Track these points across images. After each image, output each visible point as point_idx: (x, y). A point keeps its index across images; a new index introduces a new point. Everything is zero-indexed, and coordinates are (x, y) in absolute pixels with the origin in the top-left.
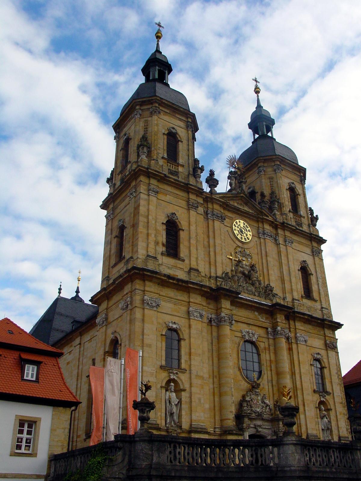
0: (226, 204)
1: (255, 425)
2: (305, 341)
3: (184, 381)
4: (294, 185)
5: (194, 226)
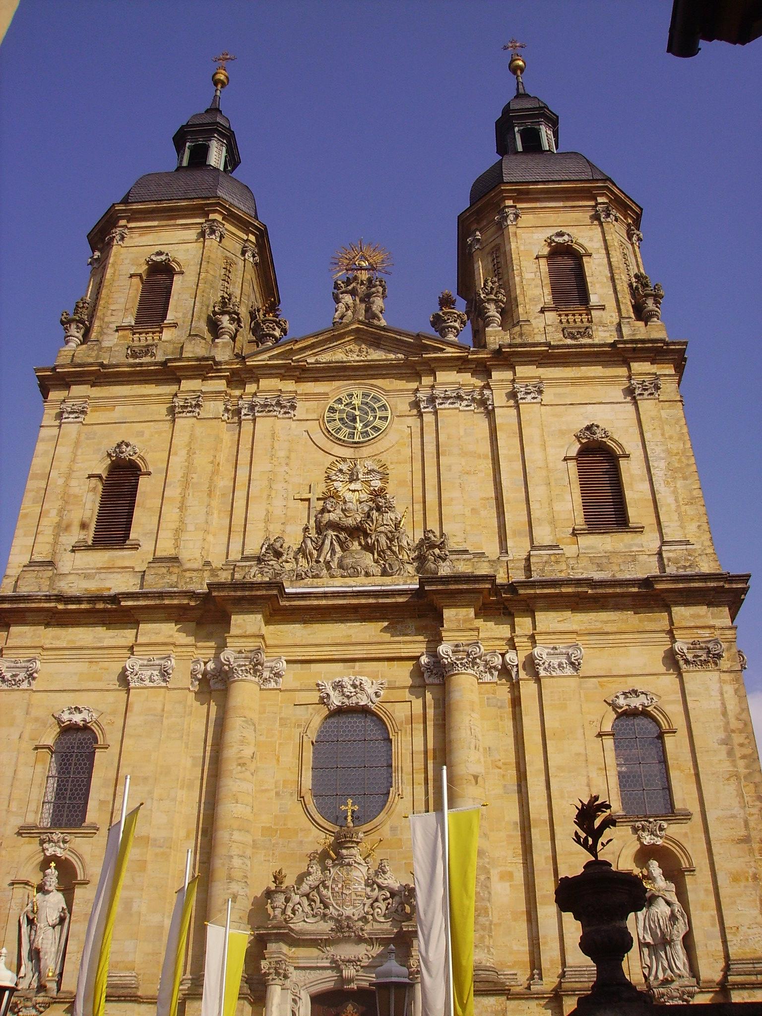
1: (334, 961)
2: (572, 664)
3: (87, 858)
4: (566, 238)
5: (183, 453)
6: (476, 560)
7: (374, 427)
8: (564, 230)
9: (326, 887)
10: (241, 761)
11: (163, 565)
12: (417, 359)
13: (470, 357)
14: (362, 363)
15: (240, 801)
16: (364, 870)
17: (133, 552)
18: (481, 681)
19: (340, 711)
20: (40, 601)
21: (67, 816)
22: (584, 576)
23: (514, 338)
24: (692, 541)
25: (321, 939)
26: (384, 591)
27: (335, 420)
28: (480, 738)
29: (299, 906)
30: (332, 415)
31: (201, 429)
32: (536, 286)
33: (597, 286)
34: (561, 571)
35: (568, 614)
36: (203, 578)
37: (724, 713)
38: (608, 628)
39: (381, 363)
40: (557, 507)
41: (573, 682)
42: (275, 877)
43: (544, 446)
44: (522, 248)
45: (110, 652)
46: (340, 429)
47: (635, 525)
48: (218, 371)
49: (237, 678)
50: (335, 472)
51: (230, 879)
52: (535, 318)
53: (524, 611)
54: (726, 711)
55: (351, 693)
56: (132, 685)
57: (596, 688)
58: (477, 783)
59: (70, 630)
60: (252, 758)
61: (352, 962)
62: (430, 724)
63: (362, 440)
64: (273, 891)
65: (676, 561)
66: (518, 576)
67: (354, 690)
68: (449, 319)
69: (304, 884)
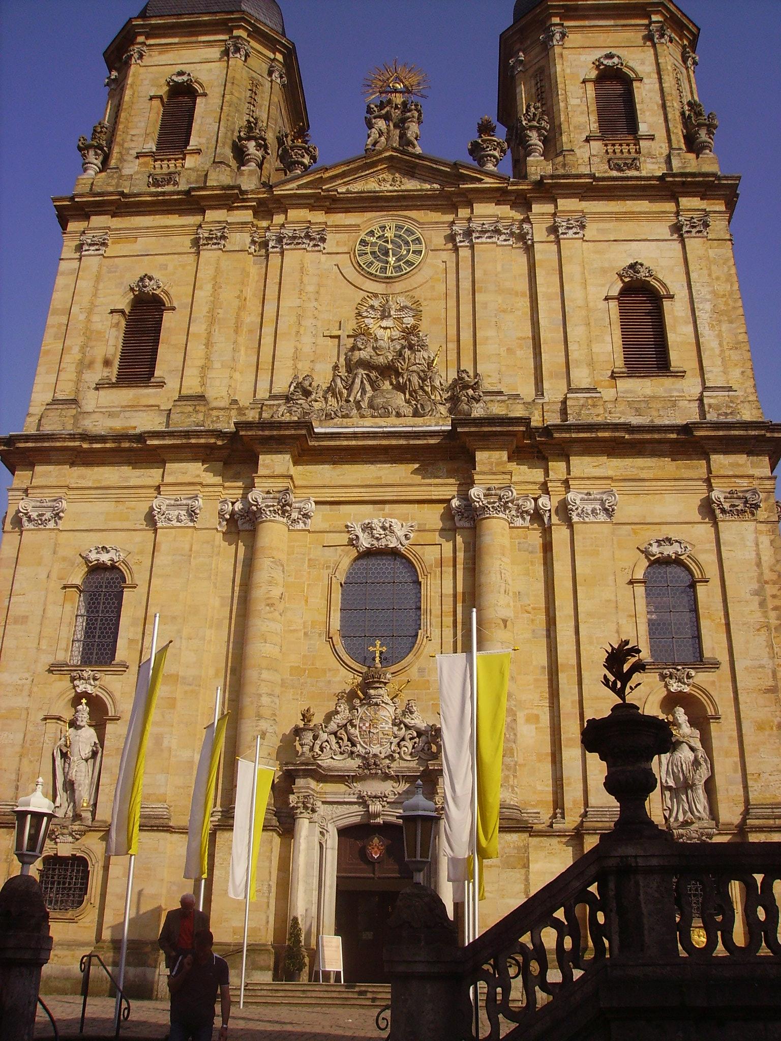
0: (325, 197)
2: (606, 510)
3: (117, 695)
4: (616, 60)
5: (209, 287)
6: (511, 401)
7: (408, 261)
8: (614, 51)
9: (354, 726)
10: (269, 602)
11: (189, 403)
12: (453, 189)
13: (509, 188)
14: (395, 194)
15: (268, 641)
16: (392, 710)
17: (158, 390)
18: (512, 525)
19: (369, 554)
20: (64, 440)
21: (97, 654)
22: (622, 421)
23: (557, 169)
24: (734, 388)
25: (348, 776)
26: (415, 432)
27: (367, 253)
28: (510, 582)
29: (326, 743)
30: (363, 248)
31: (226, 262)
32: (582, 113)
33: (648, 113)
34: (598, 415)
35: (604, 459)
36: (230, 417)
37: (759, 564)
38: (644, 475)
39: (415, 193)
40: (596, 348)
41: (606, 529)
42: (303, 715)
43: (585, 285)
44: (568, 71)
45: (136, 491)
46: (372, 263)
47: (676, 369)
48: (244, 200)
49: (265, 519)
50: (365, 308)
51: (259, 717)
52: (580, 147)
53: (558, 456)
54: (761, 562)
55: (380, 535)
56: (159, 525)
57: (629, 535)
58: (505, 626)
59: (96, 469)
60: (281, 598)
61: (378, 798)
62: (460, 567)
63: (394, 274)
64: (301, 729)
65: (717, 408)
66: (554, 419)
67: (383, 532)
68: (488, 147)
69: (332, 723)
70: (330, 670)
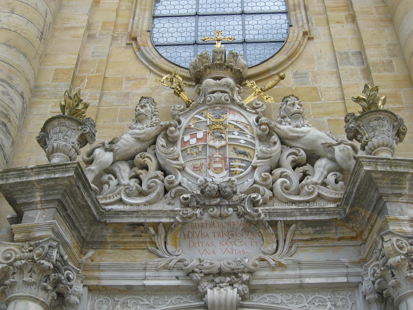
25: (156, 226)
70: (128, 79)
